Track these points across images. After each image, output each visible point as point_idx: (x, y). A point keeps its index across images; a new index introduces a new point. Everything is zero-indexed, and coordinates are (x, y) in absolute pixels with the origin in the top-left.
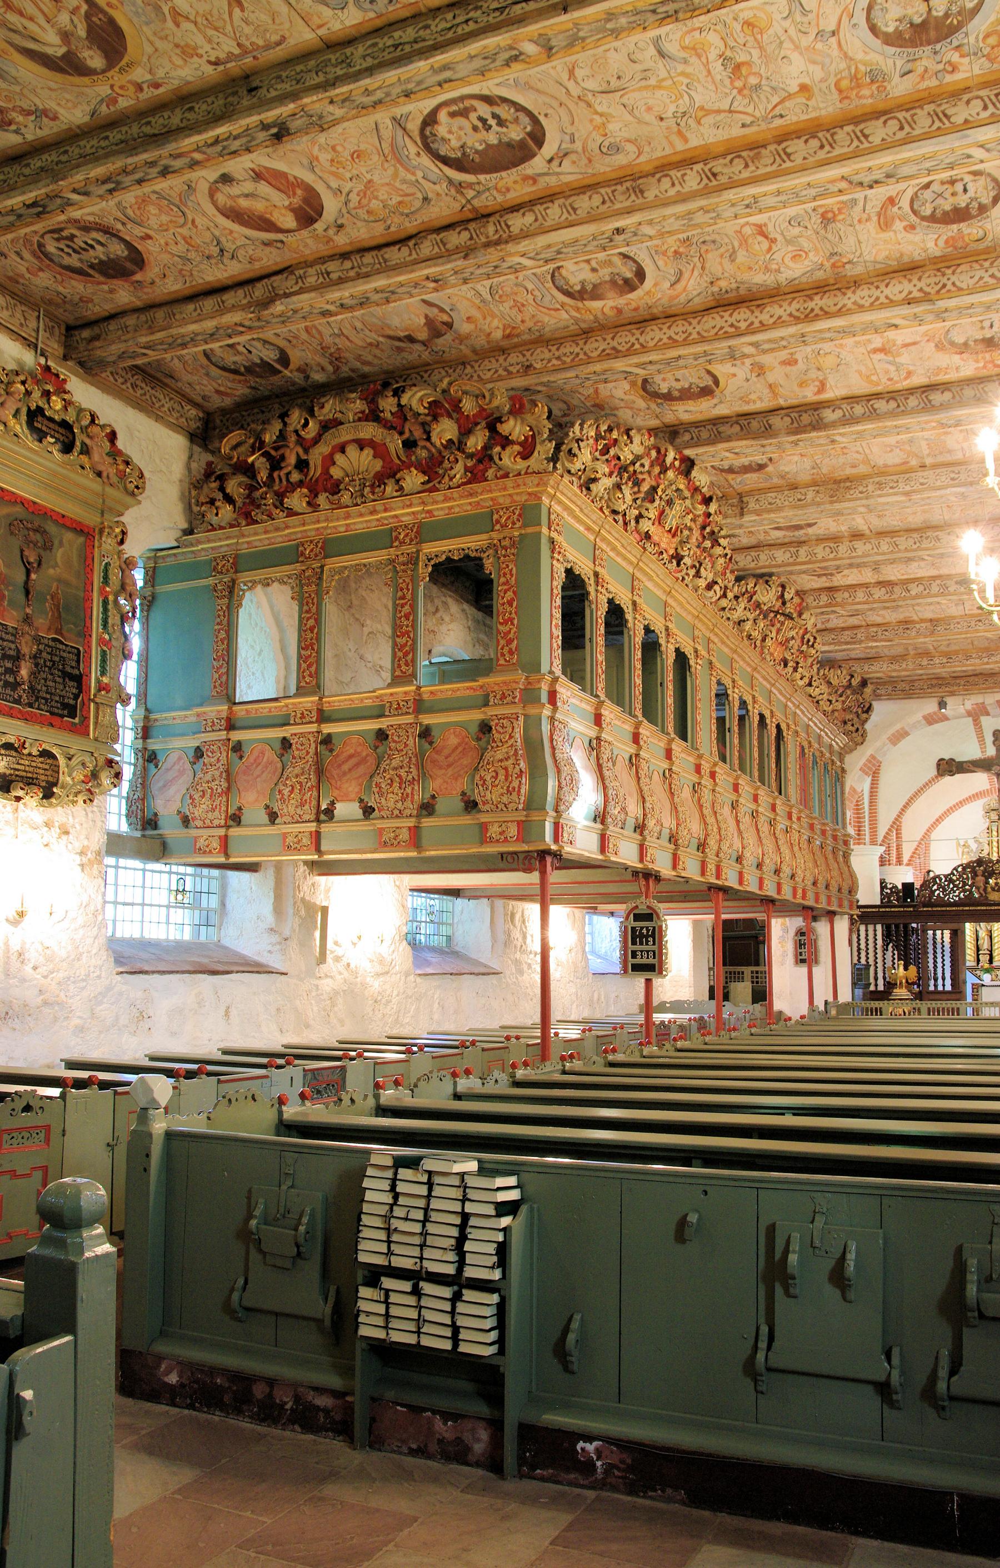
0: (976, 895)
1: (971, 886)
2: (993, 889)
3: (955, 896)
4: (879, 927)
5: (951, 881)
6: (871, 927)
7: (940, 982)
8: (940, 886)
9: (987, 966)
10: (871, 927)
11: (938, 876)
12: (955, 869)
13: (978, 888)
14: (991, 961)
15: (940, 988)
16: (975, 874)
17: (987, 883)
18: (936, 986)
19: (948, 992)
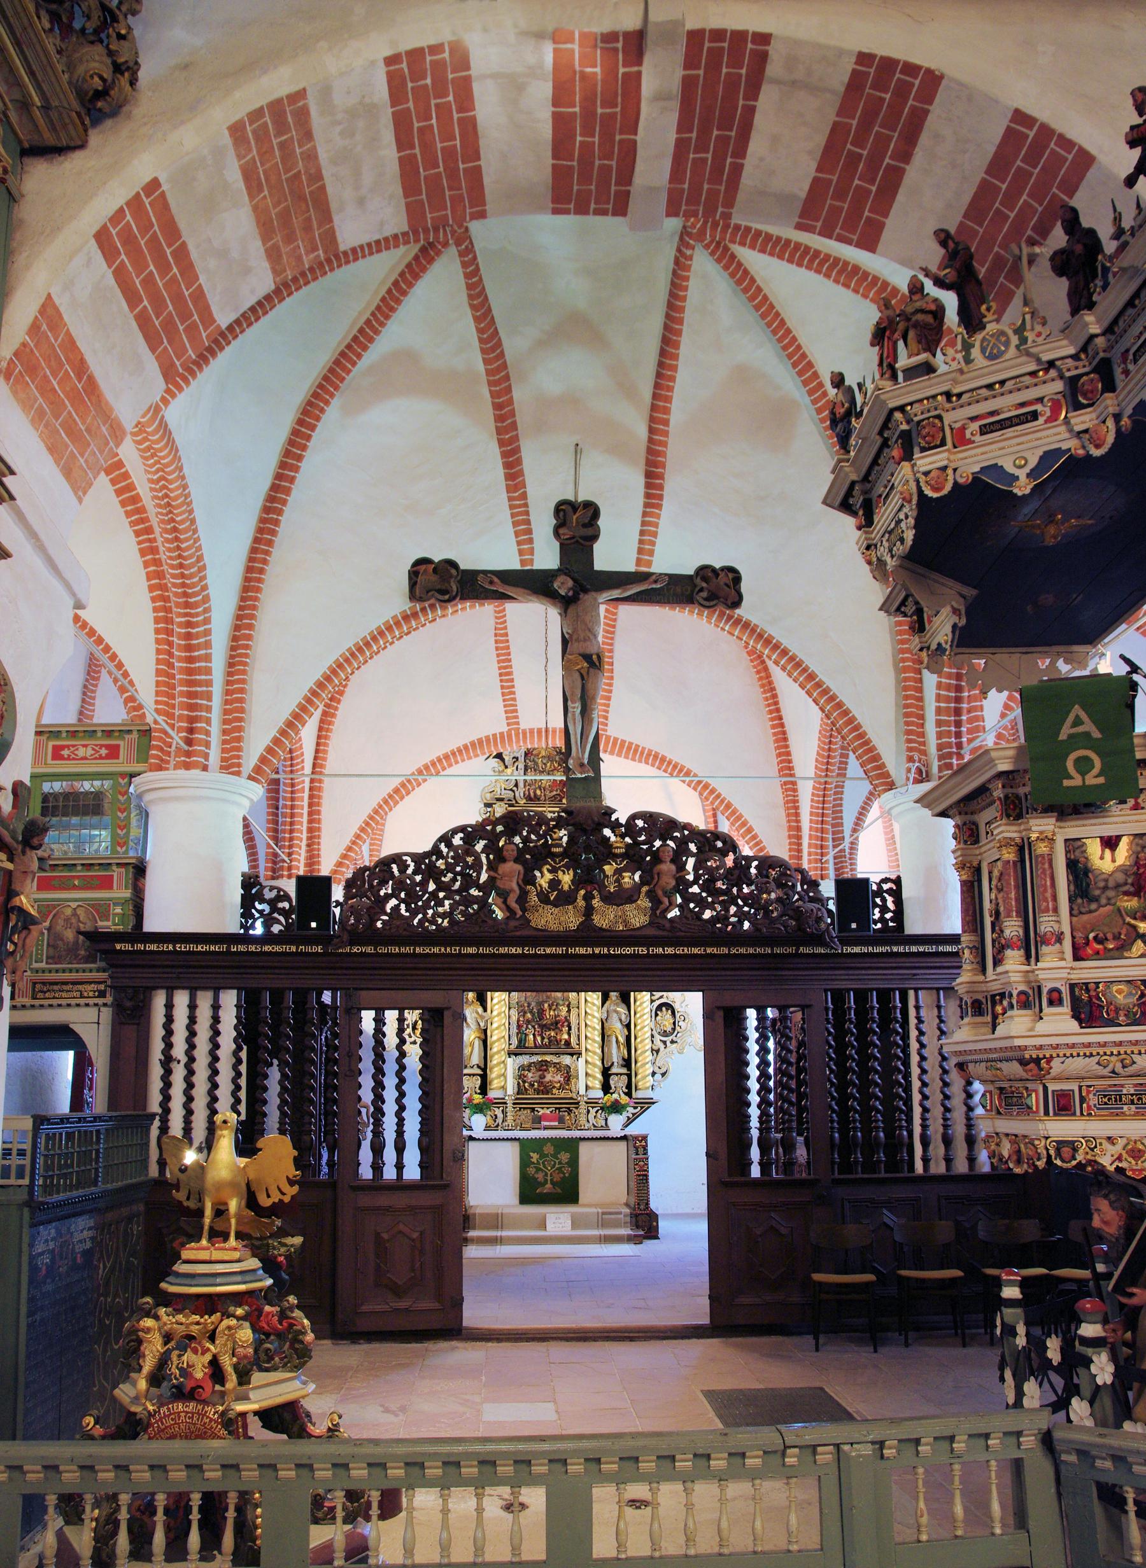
0: (499, 914)
1: (486, 888)
2: (544, 898)
3: (442, 912)
4: (229, 999)
5: (432, 873)
6: (204, 1001)
7: (390, 1155)
8: (400, 885)
9: (478, 1098)
10: (204, 1001)
11: (397, 858)
12: (446, 839)
13: (503, 895)
14: (483, 1089)
15: (390, 1173)
16: (498, 857)
17: (530, 880)
18: (377, 1167)
19: (412, 1186)
